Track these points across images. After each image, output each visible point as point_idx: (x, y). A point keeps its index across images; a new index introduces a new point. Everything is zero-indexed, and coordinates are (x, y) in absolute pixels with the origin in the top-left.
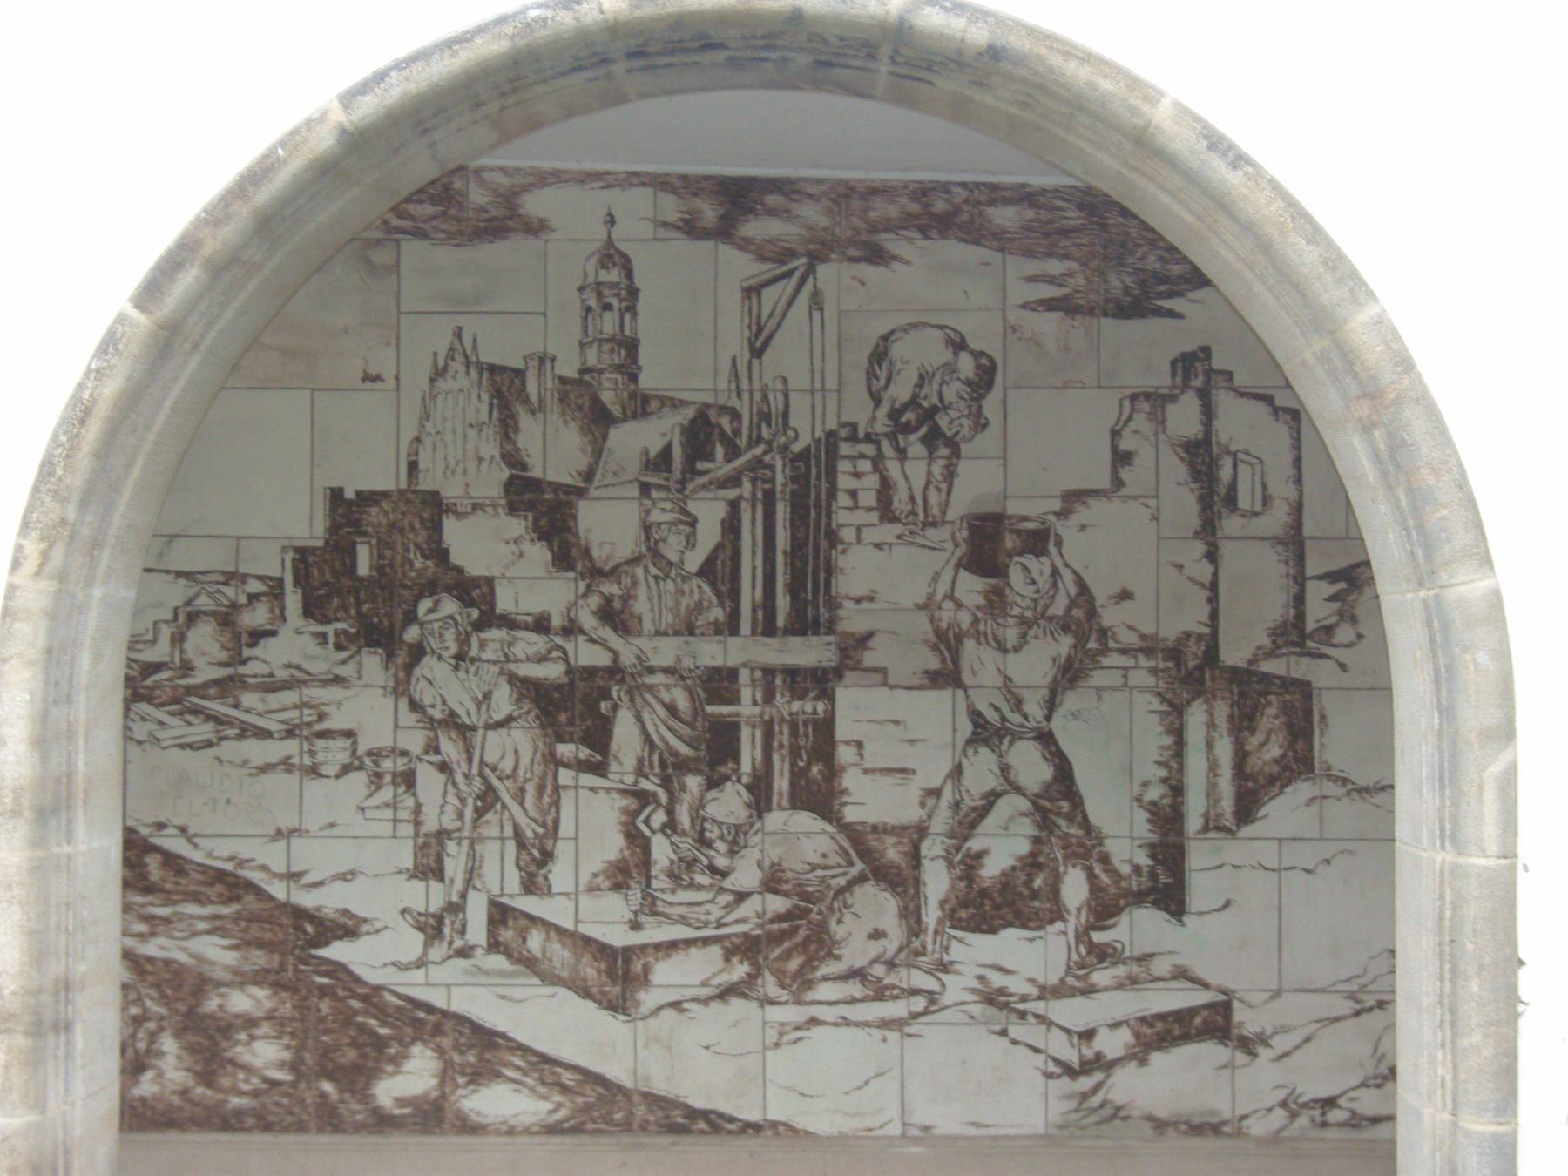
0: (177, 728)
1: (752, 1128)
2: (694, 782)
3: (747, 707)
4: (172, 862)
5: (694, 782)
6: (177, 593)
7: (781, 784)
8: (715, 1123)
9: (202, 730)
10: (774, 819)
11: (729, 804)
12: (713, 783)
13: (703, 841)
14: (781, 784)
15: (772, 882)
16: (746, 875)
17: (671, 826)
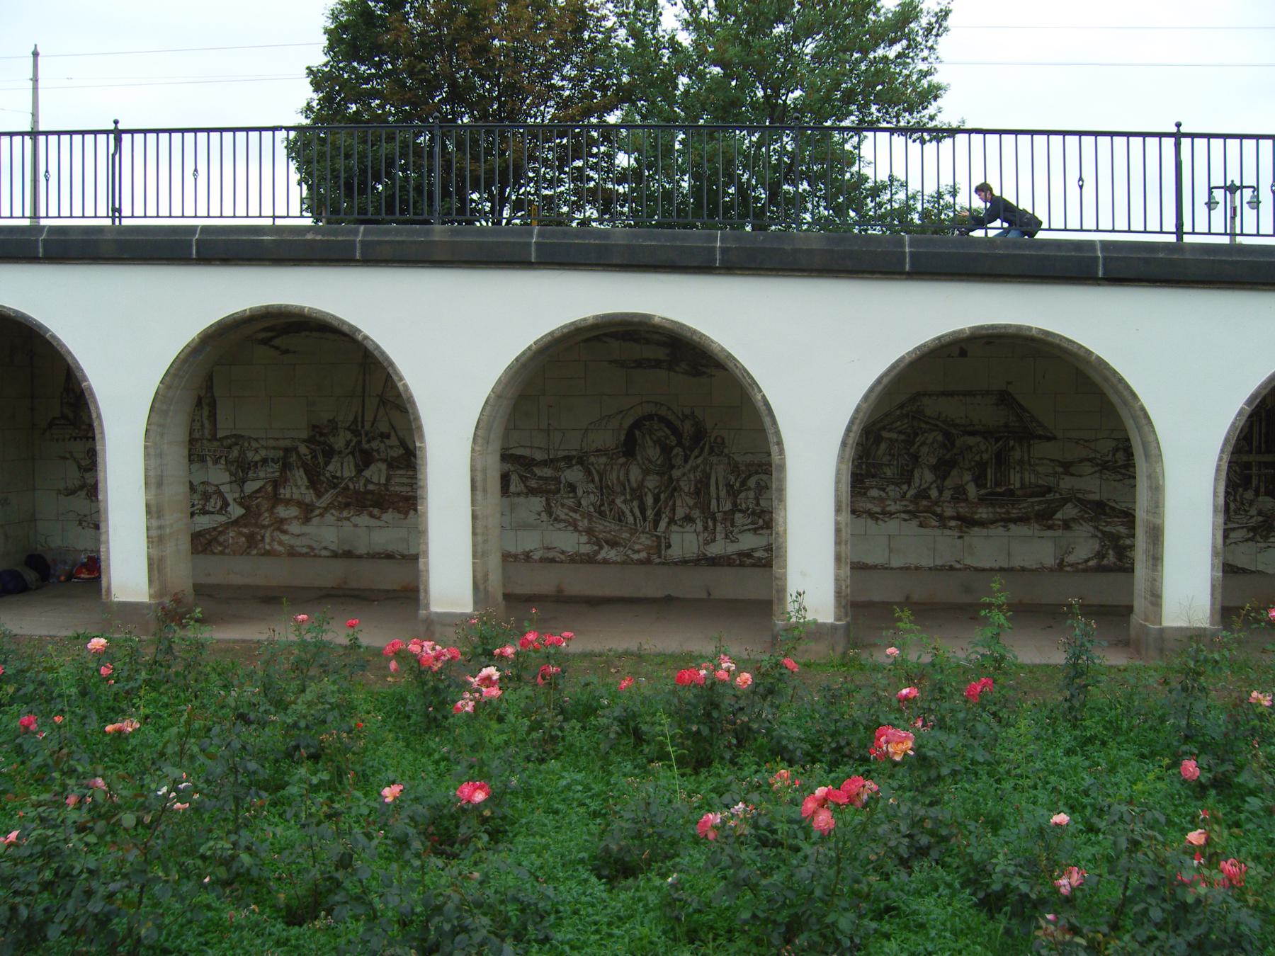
0: (1114, 476)
1: (1252, 572)
2: (1241, 490)
3: (1254, 471)
4: (1113, 509)
5: (1241, 490)
6: (1113, 444)
7: (1262, 490)
8: (1244, 571)
9: (1120, 477)
10: (1260, 499)
11: (1249, 495)
12: (1246, 490)
13: (1243, 504)
14: (1262, 490)
15: (1260, 513)
16: (1253, 512)
17: (1235, 500)
